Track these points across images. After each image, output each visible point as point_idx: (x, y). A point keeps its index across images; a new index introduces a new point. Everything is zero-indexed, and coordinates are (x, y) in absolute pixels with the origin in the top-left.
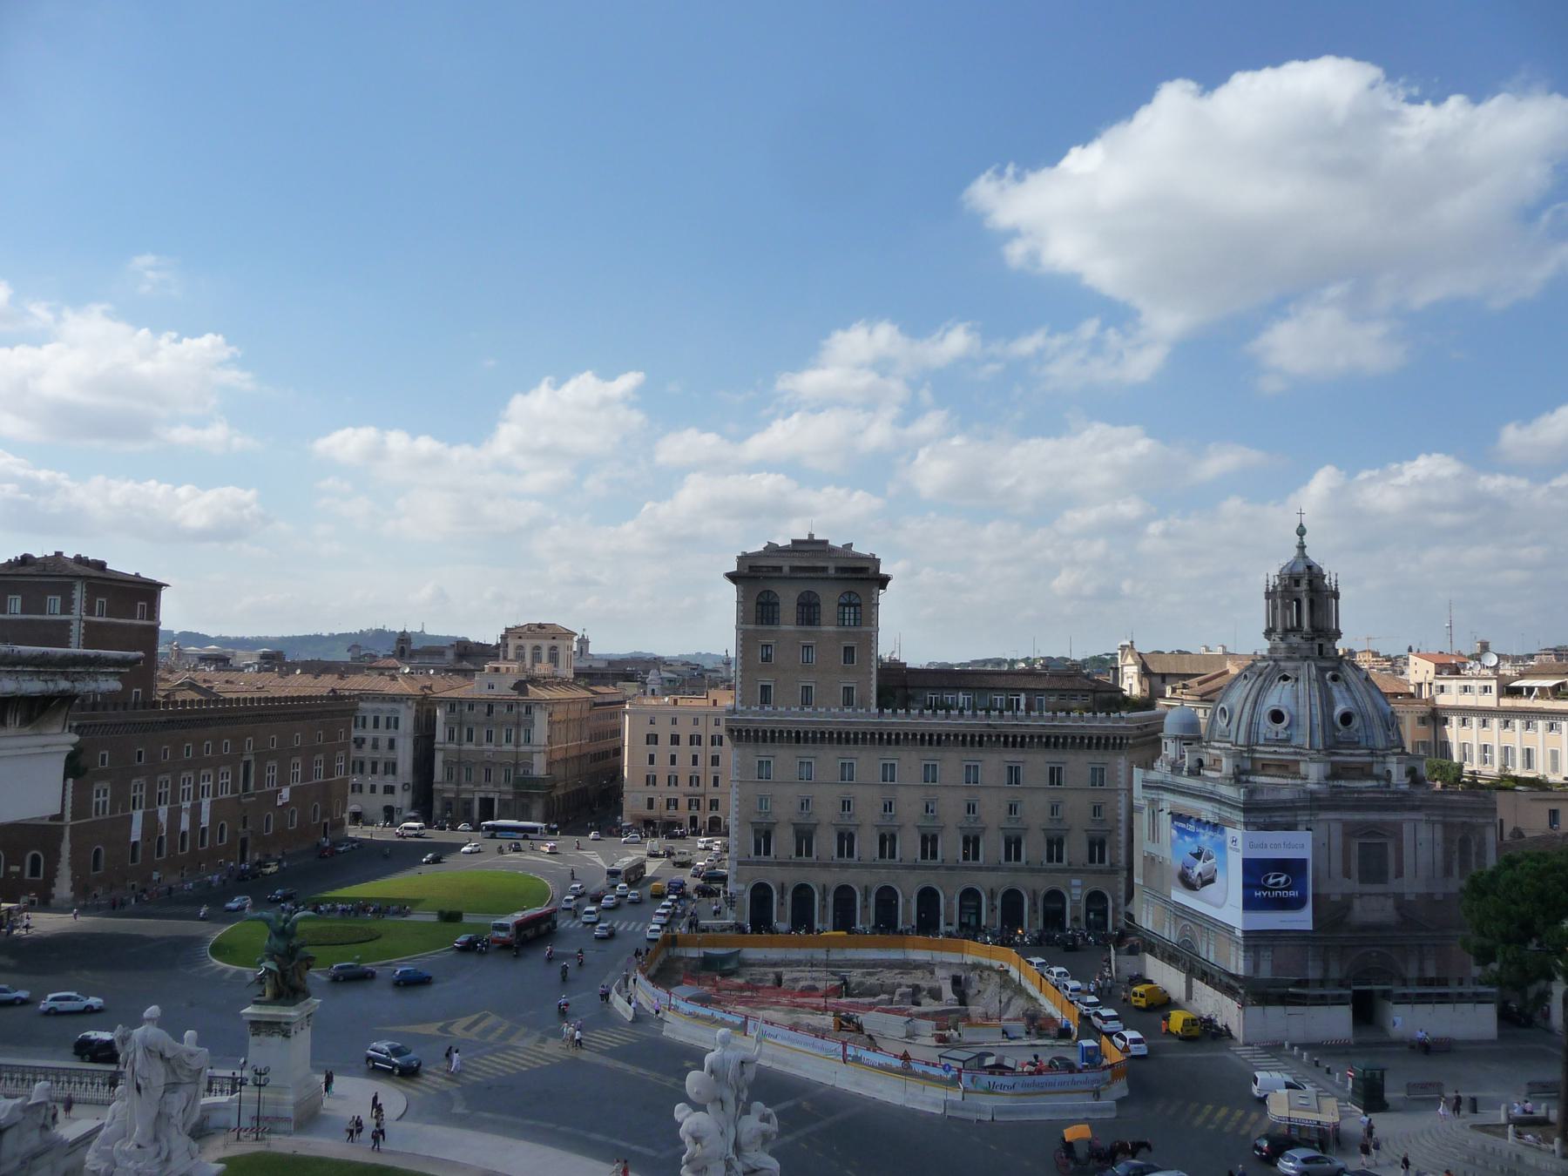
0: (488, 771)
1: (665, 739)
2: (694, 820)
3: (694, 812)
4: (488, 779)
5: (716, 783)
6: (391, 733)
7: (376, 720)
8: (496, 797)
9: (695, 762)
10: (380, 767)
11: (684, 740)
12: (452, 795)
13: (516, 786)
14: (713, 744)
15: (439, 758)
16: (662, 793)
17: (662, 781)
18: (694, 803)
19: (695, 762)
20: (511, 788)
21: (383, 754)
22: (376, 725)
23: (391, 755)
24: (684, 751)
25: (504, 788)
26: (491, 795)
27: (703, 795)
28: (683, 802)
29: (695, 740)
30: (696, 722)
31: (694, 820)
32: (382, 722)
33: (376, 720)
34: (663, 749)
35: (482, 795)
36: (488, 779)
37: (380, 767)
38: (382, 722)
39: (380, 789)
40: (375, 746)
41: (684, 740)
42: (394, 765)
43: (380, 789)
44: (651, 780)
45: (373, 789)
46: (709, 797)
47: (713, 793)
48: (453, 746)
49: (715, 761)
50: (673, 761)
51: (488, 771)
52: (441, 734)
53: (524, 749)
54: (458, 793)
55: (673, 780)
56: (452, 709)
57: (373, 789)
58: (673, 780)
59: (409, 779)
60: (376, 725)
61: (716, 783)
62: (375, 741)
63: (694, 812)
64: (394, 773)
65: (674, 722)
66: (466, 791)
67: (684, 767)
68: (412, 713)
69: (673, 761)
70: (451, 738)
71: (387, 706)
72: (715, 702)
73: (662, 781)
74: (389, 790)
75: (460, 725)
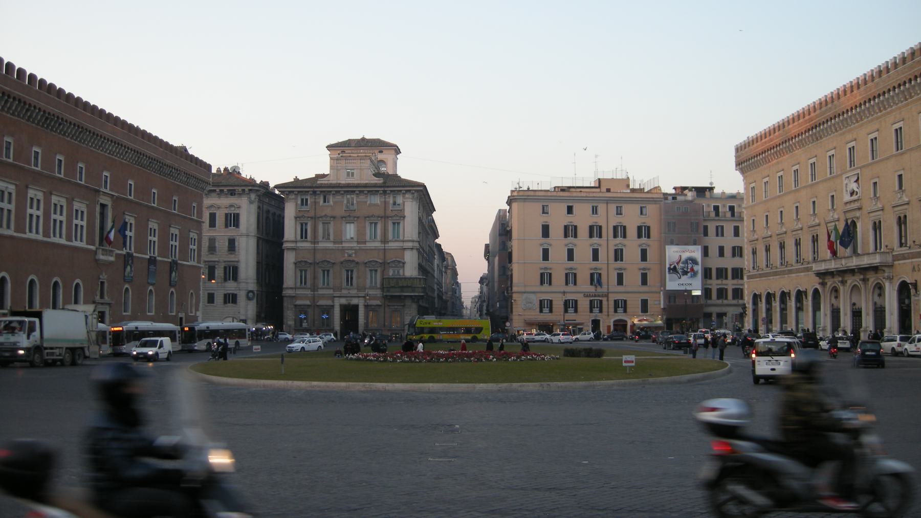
0: (350, 272)
1: (556, 231)
2: (596, 324)
3: (596, 314)
4: (349, 280)
5: (620, 281)
6: (232, 232)
7: (213, 217)
8: (361, 303)
9: (596, 256)
10: (219, 272)
11: (583, 232)
12: (308, 303)
13: (382, 288)
14: (615, 236)
15: (289, 259)
16: (557, 292)
17: (559, 278)
18: (595, 305)
19: (596, 256)
20: (378, 293)
21: (222, 256)
22: (212, 224)
23: (232, 258)
24: (583, 245)
25: (371, 292)
26: (355, 301)
27: (607, 296)
28: (584, 304)
29: (595, 231)
30: (595, 210)
31: (596, 324)
32: (220, 220)
33: (213, 217)
34: (558, 245)
35: (343, 301)
36: (349, 280)
37: (219, 272)
38: (220, 220)
39: (219, 299)
40: (212, 249)
41: (583, 232)
42: (235, 270)
43: (219, 299)
44: (545, 278)
45: (211, 298)
46: (613, 297)
47: (617, 293)
48: (307, 245)
49: (618, 255)
50: (571, 255)
51: (350, 272)
52: (290, 230)
53: (392, 245)
54: (314, 298)
55: (571, 278)
56: (304, 202)
57: (211, 298)
58: (571, 278)
59: (253, 286)
60: (212, 224)
61: (620, 281)
62: (212, 241)
63: (596, 314)
64: (235, 278)
65: (570, 210)
66: (323, 297)
67: (583, 264)
68: (254, 208)
69: (571, 255)
70: (304, 235)
71: (225, 201)
72: (608, 190)
73: (559, 278)
74: (231, 299)
75: (315, 218)
